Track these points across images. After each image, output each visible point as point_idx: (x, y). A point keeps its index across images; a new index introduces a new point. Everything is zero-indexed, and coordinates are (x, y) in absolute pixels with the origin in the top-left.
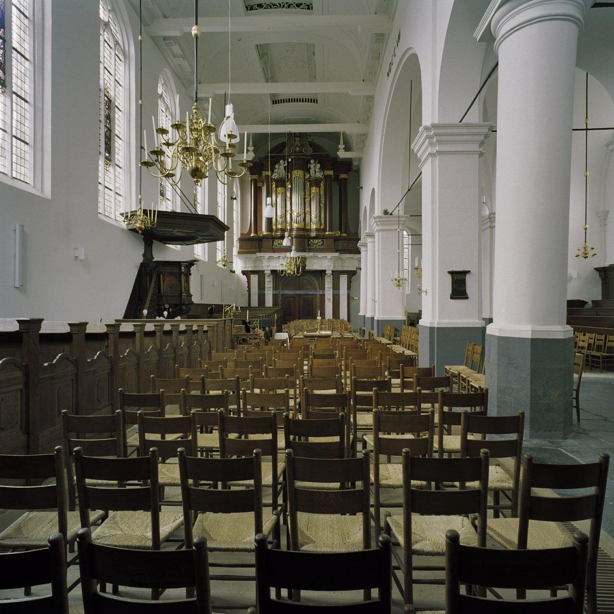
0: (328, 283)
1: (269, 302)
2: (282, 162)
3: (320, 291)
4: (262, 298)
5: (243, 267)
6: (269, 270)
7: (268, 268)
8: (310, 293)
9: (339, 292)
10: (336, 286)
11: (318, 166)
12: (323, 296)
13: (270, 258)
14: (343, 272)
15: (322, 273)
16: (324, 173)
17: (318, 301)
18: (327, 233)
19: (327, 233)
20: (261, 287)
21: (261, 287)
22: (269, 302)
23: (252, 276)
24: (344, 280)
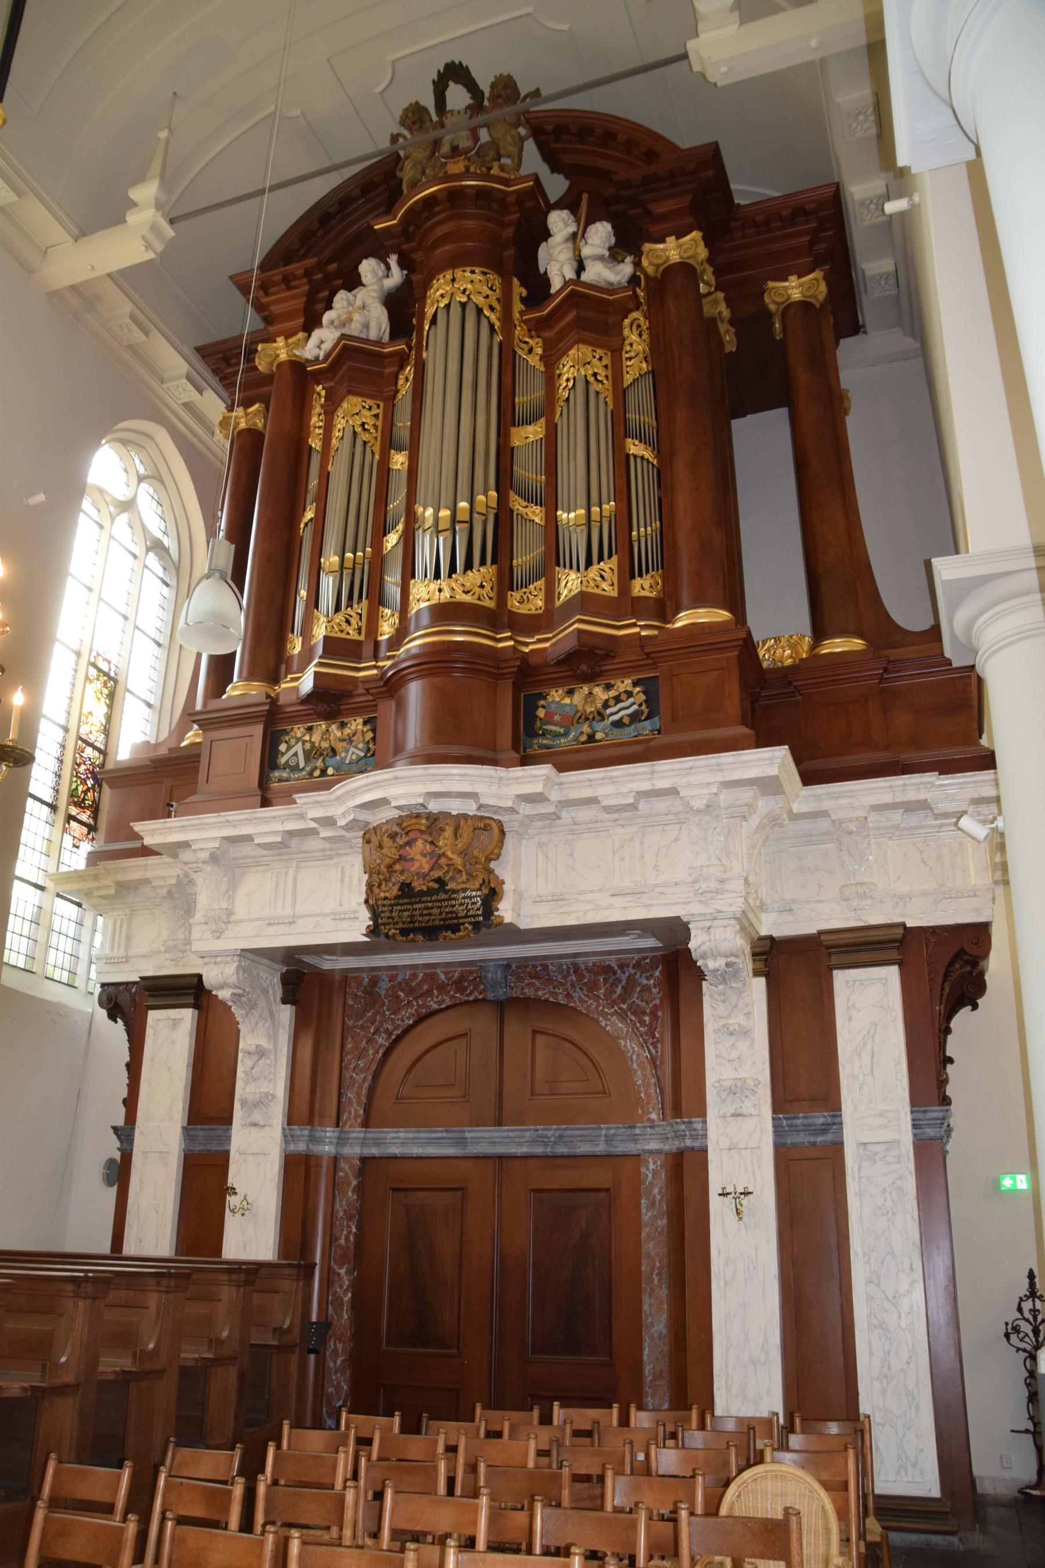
0: (736, 1037)
1: (251, 1234)
2: (368, 268)
3: (664, 1128)
4: (204, 1183)
5: (112, 962)
6: (226, 953)
7: (218, 934)
8: (584, 1148)
9: (836, 1124)
10: (803, 1074)
11: (601, 234)
12: (687, 1169)
13: (228, 859)
14: (864, 946)
15: (668, 967)
16: (637, 264)
17: (652, 1216)
18: (683, 620)
19: (683, 620)
20: (210, 1103)
21: (210, 1103)
22: (251, 1234)
23: (153, 1015)
24: (869, 1008)
